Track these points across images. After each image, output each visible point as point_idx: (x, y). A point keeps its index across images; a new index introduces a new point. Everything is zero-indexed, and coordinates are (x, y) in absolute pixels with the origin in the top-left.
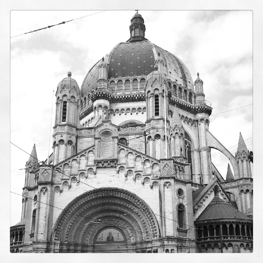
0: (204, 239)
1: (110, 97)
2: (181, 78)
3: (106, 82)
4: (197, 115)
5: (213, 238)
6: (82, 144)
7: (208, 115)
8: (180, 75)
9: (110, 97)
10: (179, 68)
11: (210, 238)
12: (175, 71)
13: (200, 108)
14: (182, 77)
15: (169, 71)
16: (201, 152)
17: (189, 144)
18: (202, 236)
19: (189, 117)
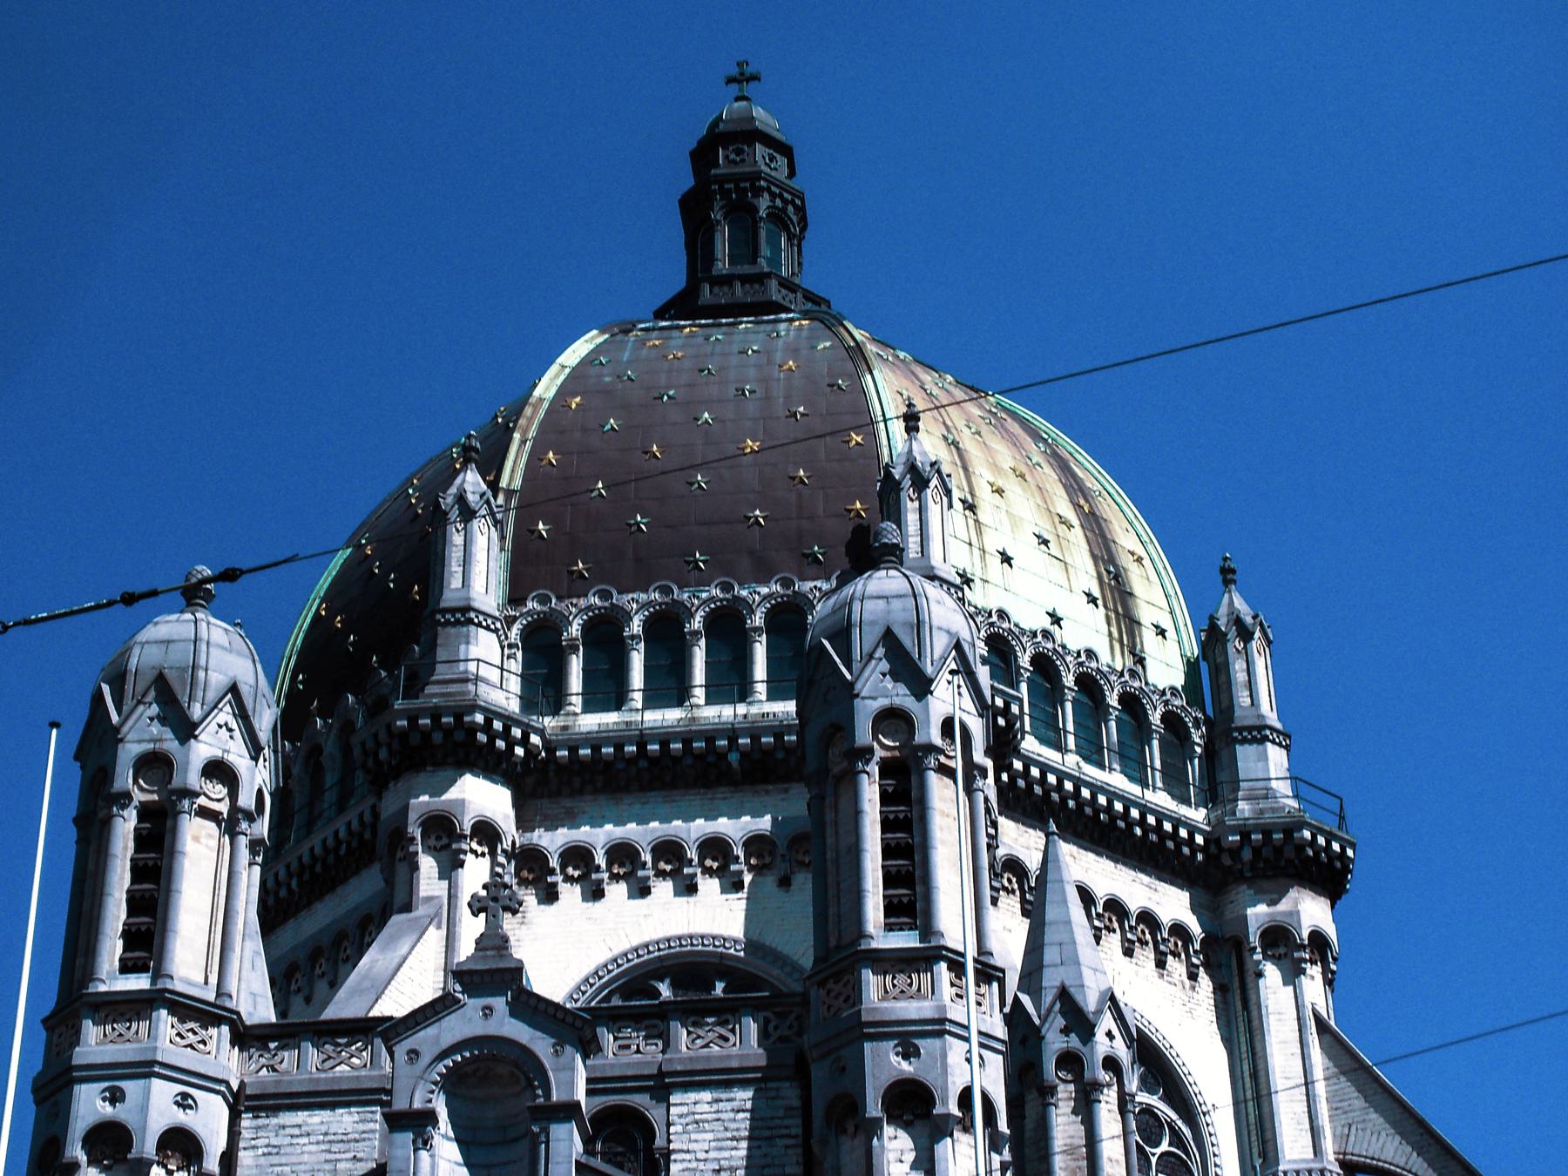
2: (1092, 600)
3: (487, 628)
4: (1232, 896)
6: (275, 1160)
8: (1086, 576)
10: (1075, 521)
12: (1045, 542)
14: (1096, 593)
15: (993, 542)
19: (1166, 916)
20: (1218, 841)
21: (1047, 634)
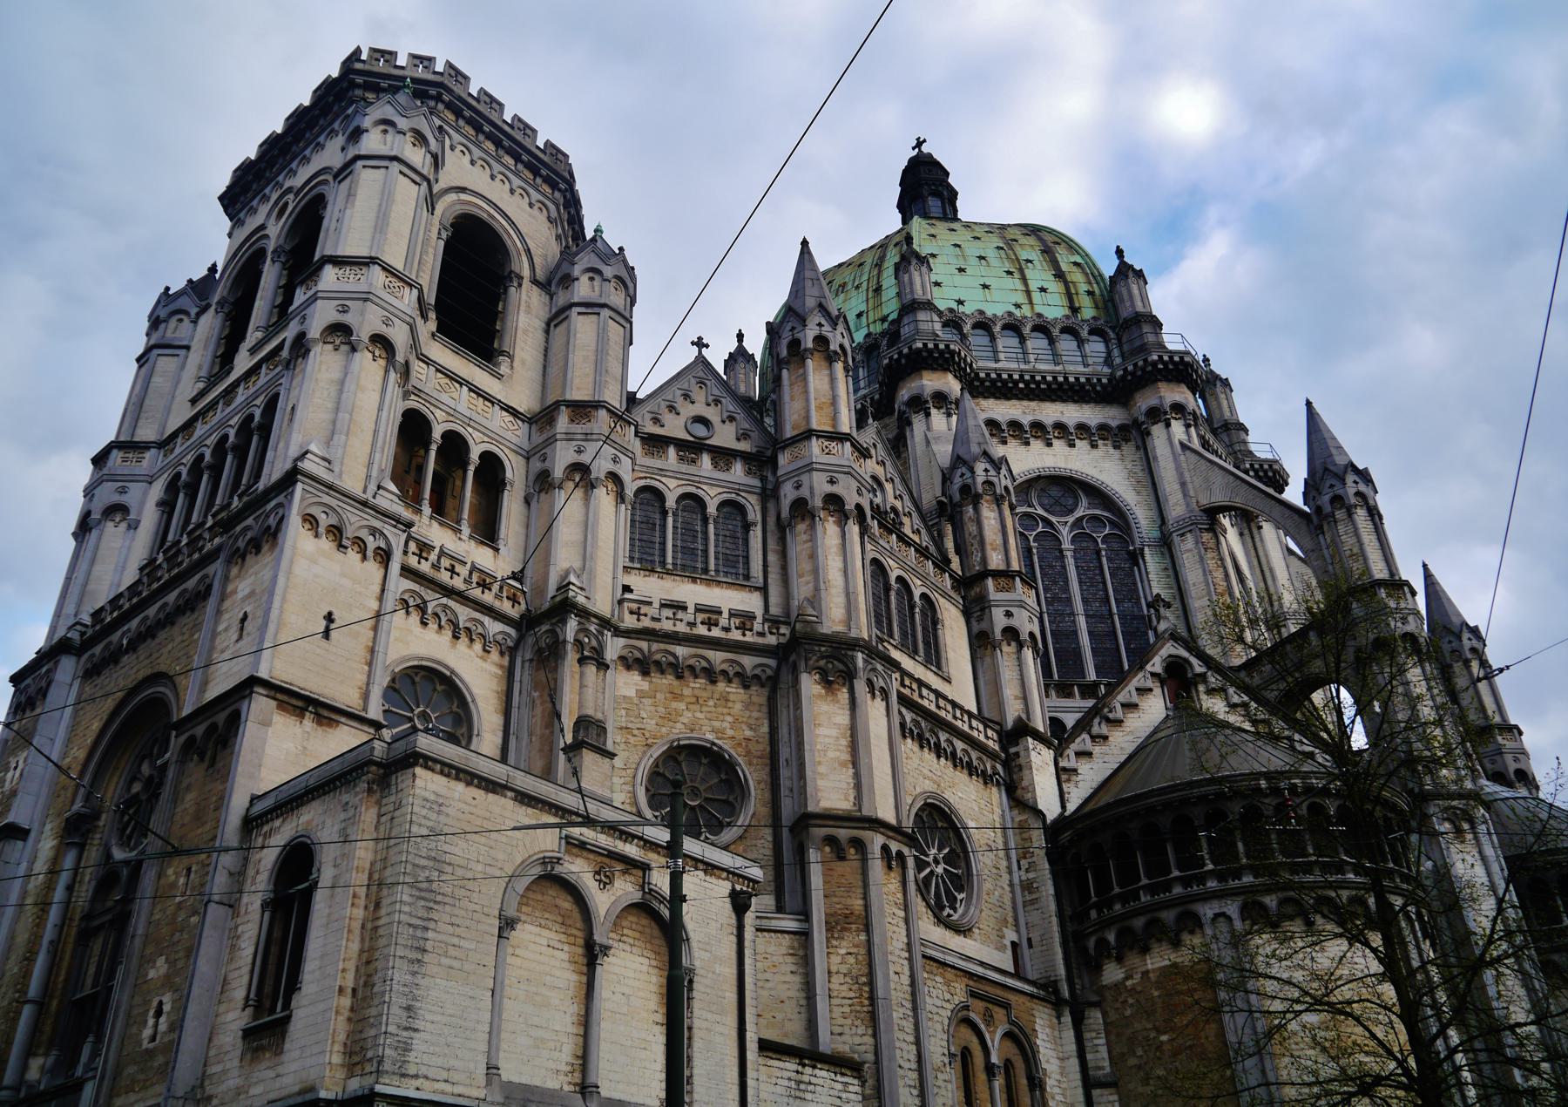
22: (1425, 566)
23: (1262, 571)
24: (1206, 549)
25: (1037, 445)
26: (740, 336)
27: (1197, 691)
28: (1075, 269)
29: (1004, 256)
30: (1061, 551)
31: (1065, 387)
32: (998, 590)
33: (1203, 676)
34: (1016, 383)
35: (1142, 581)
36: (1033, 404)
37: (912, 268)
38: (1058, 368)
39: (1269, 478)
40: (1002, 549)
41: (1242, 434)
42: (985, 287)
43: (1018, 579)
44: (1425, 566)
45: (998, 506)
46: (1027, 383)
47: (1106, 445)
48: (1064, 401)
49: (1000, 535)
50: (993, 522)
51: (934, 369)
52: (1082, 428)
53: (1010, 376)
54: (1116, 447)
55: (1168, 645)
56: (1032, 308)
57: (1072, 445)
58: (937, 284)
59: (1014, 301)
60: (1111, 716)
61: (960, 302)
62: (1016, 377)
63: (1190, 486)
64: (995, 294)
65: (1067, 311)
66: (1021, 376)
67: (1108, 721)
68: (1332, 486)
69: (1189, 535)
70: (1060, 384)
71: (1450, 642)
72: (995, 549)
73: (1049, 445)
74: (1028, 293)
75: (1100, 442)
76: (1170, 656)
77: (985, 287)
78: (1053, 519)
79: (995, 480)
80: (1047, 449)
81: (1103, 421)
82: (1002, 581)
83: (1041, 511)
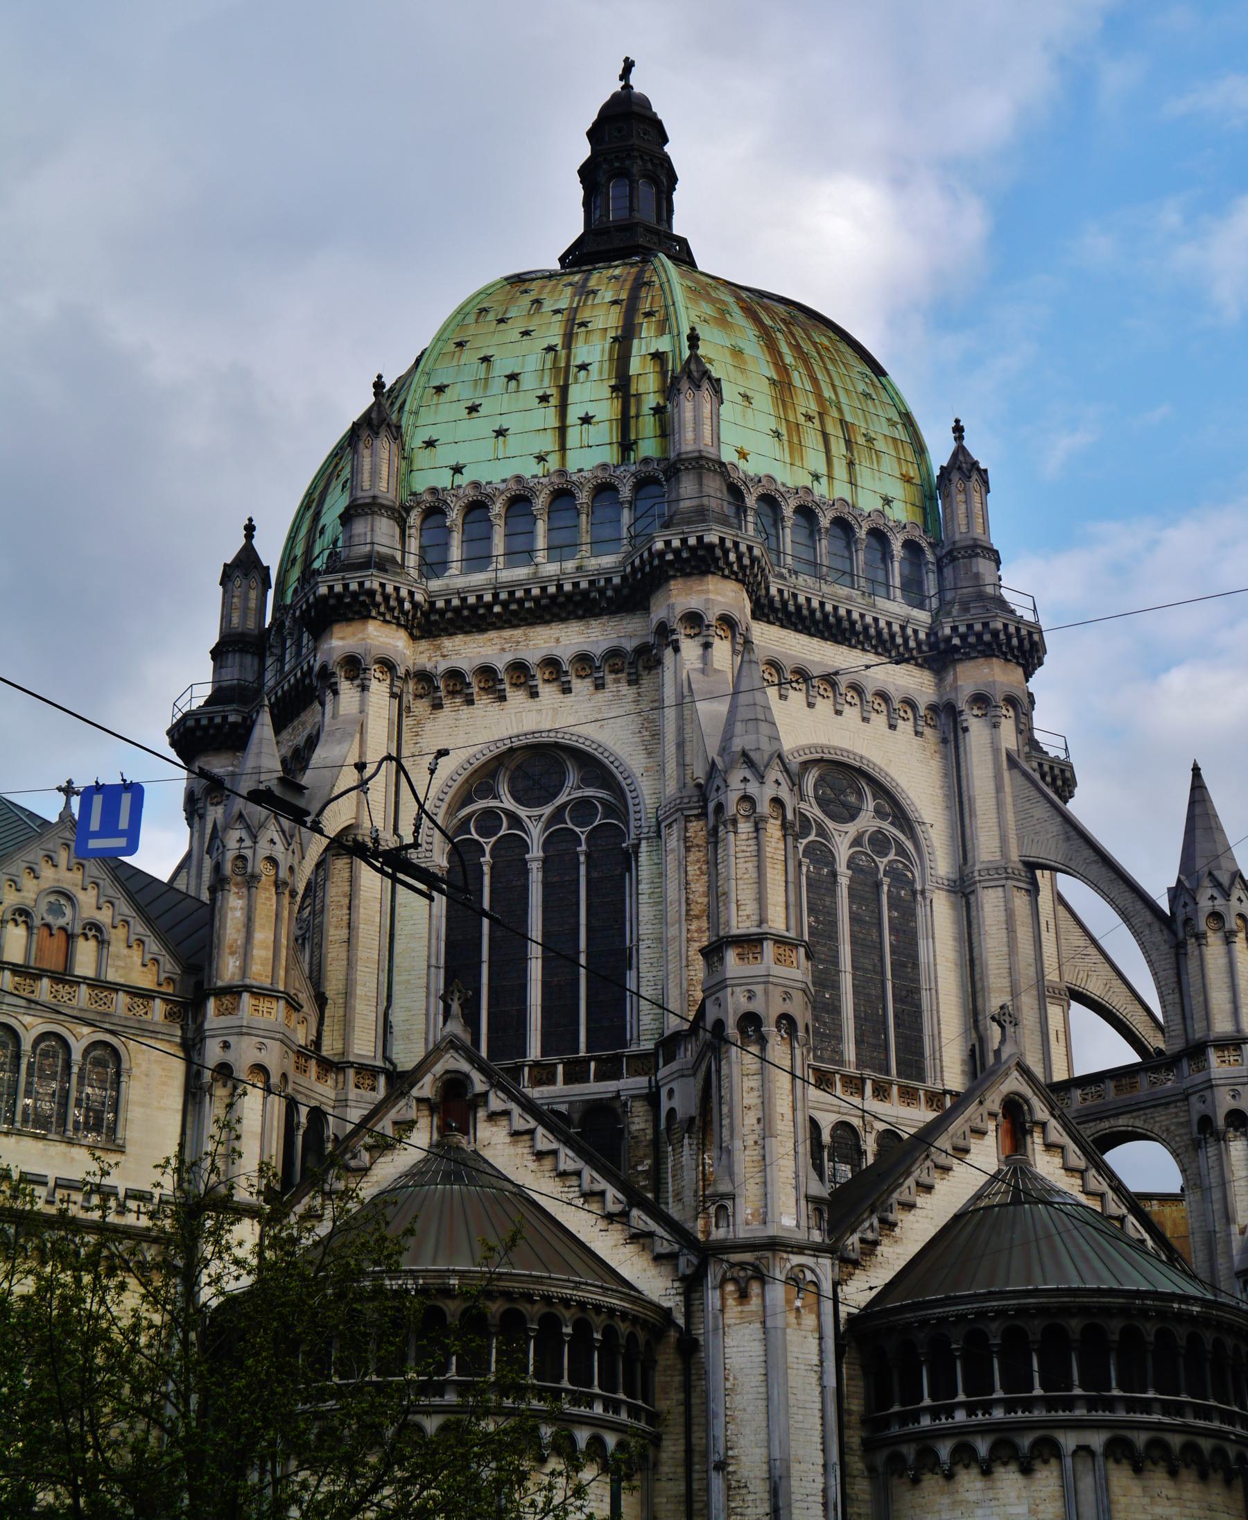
0: (935, 1413)
1: (407, 606)
5: (1028, 1404)
7: (1020, 671)
9: (407, 606)
11: (1010, 1406)
13: (962, 629)
16: (972, 898)
17: (902, 851)
18: (955, 1395)
20: (936, 634)
21: (808, 490)
22: (1196, 770)
23: (961, 803)
24: (688, 849)
25: (516, 698)
26: (250, 529)
27: (475, 1118)
28: (650, 366)
29: (549, 365)
30: (525, 862)
31: (561, 599)
32: (220, 1013)
33: (486, 1094)
34: (489, 607)
35: (631, 896)
36: (518, 633)
37: (361, 445)
38: (570, 565)
39: (988, 644)
40: (241, 951)
41: (983, 566)
42: (501, 433)
43: (246, 996)
44: (1196, 770)
45: (249, 888)
46: (505, 604)
47: (617, 681)
48: (563, 620)
49: (242, 935)
50: (238, 914)
51: (349, 620)
52: (583, 659)
53: (480, 598)
54: (630, 683)
55: (448, 1056)
56: (563, 458)
57: (566, 690)
58: (430, 444)
59: (536, 451)
60: (353, 1163)
61: (457, 470)
62: (488, 598)
63: (688, 748)
64: (513, 444)
65: (610, 455)
66: (496, 596)
67: (348, 1169)
68: (745, 780)
69: (675, 826)
70: (553, 598)
71: (1212, 898)
72: (232, 953)
73: (534, 694)
74: (562, 430)
75: (610, 678)
76: (447, 1072)
77: (501, 433)
78: (523, 812)
79: (248, 853)
80: (531, 704)
81: (615, 643)
82: (227, 1000)
83: (508, 803)
